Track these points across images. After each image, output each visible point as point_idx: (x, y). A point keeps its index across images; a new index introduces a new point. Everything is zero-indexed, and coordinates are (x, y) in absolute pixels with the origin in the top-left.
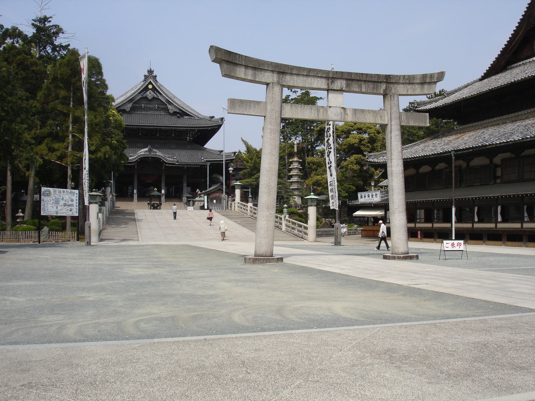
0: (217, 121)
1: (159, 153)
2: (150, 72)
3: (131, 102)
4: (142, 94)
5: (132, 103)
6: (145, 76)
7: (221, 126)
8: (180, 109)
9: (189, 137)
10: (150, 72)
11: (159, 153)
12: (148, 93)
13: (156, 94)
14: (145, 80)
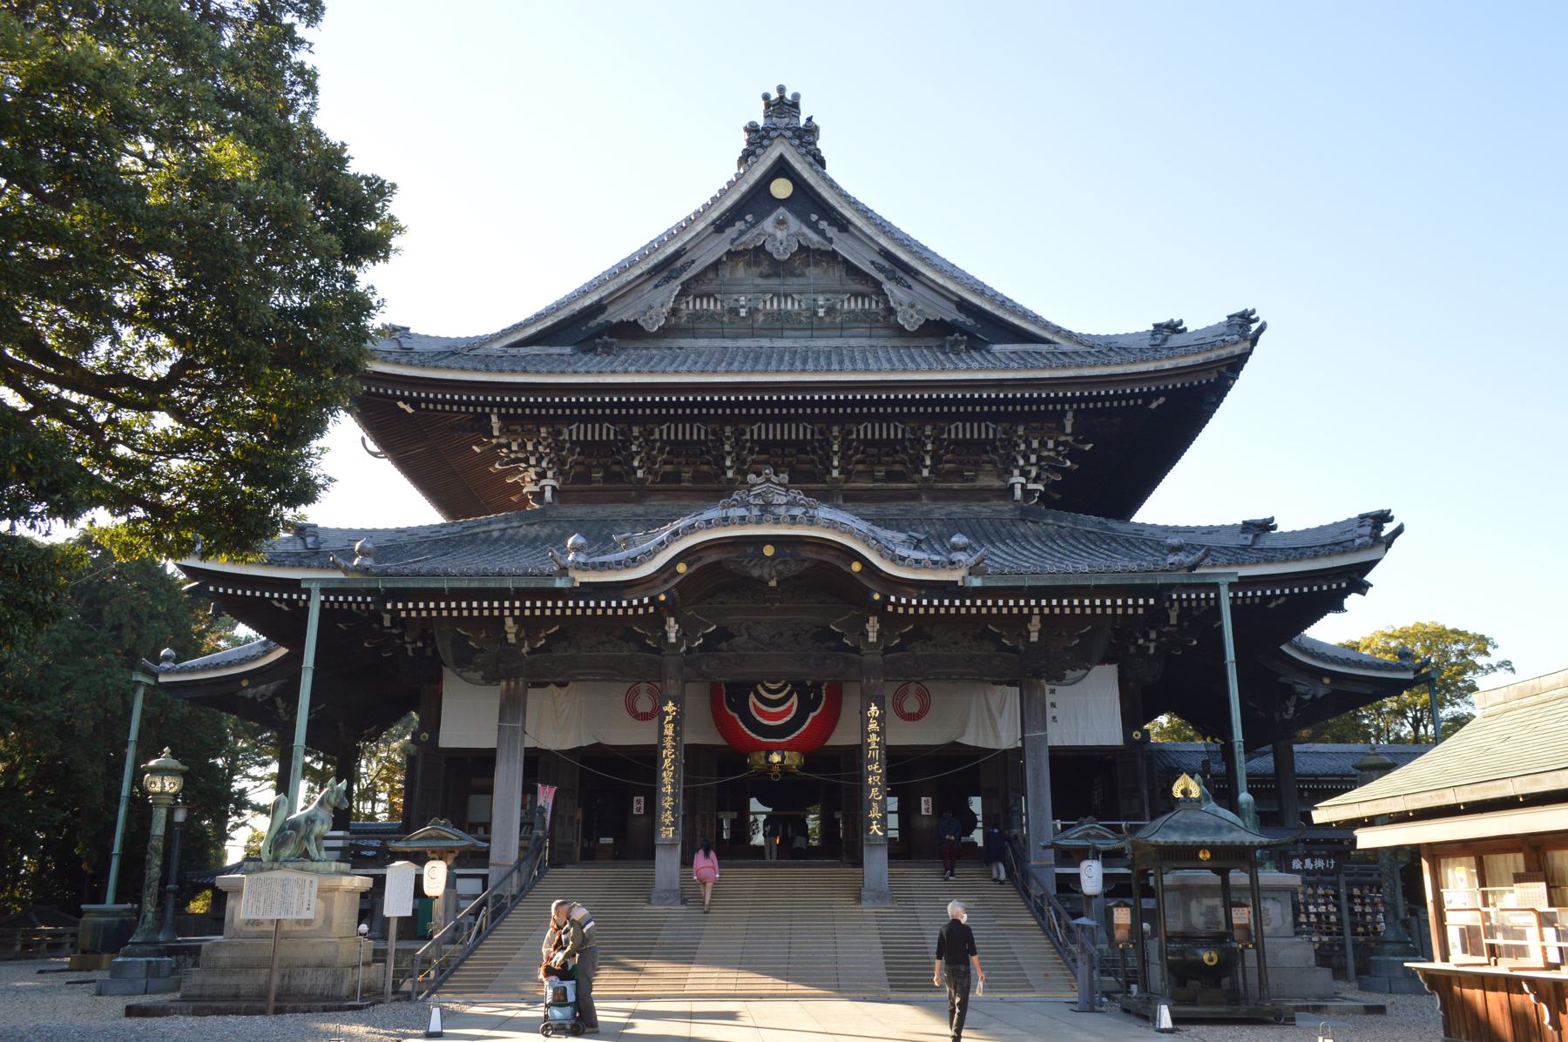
0: (1205, 341)
1: (834, 524)
2: (782, 106)
3: (667, 280)
4: (731, 232)
5: (675, 286)
6: (752, 129)
7: (1236, 364)
8: (963, 305)
9: (1024, 473)
10: (782, 106)
11: (834, 524)
12: (768, 224)
13: (813, 226)
14: (746, 157)
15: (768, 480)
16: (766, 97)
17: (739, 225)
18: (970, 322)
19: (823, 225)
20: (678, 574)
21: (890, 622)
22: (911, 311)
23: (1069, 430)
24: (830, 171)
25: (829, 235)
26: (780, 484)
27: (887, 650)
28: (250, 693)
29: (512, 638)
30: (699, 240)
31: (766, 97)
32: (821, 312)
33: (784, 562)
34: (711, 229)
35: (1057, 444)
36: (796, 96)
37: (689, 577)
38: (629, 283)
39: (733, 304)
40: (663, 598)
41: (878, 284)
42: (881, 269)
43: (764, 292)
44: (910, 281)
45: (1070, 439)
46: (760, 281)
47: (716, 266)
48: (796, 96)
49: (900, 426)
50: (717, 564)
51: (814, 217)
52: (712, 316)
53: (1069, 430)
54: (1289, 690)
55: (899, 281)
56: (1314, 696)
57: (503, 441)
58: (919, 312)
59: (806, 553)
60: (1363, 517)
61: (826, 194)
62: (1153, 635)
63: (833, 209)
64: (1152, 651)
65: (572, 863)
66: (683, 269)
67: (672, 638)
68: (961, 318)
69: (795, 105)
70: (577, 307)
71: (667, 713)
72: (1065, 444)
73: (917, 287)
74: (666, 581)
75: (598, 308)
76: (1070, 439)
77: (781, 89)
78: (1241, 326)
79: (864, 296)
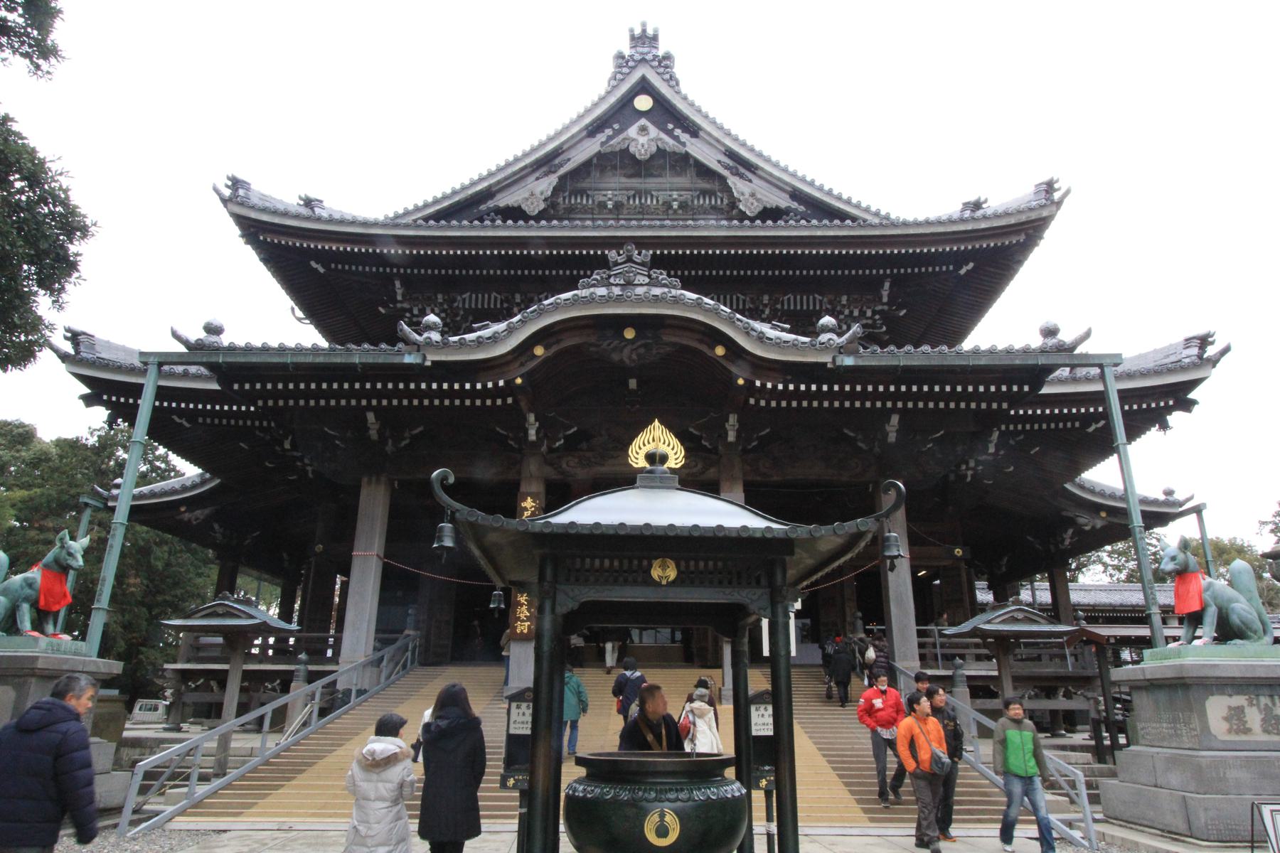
3: (546, 174)
4: (601, 137)
5: (553, 180)
8: (796, 195)
10: (644, 39)
12: (632, 131)
13: (670, 133)
14: (616, 79)
15: (630, 259)
16: (632, 30)
17: (609, 132)
18: (802, 208)
19: (678, 132)
20: (535, 356)
21: (750, 421)
22: (751, 200)
23: (885, 299)
24: (684, 88)
25: (683, 140)
26: (643, 264)
27: (745, 451)
28: (187, 516)
29: (373, 434)
30: (574, 142)
31: (632, 30)
32: (675, 205)
33: (645, 346)
34: (584, 133)
35: (874, 313)
36: (656, 30)
37: (546, 361)
38: (515, 174)
39: (602, 199)
40: (519, 381)
41: (723, 179)
42: (727, 167)
43: (627, 189)
44: (750, 175)
45: (886, 308)
46: (623, 180)
47: (587, 165)
48: (656, 30)
49: (742, 297)
50: (577, 348)
51: (670, 126)
52: (585, 210)
53: (885, 299)
54: (1071, 522)
55: (737, 174)
56: (1093, 527)
57: (406, 305)
58: (758, 200)
59: (669, 338)
60: (1188, 340)
61: (681, 105)
62: (972, 464)
63: (686, 118)
64: (969, 479)
65: (447, 664)
66: (561, 165)
67: (532, 434)
68: (795, 205)
69: (655, 38)
70: (471, 192)
71: (526, 509)
72: (879, 312)
73: (755, 180)
74: (522, 365)
75: (488, 194)
76: (886, 308)
77: (644, 25)
78: (1047, 192)
79: (711, 193)
